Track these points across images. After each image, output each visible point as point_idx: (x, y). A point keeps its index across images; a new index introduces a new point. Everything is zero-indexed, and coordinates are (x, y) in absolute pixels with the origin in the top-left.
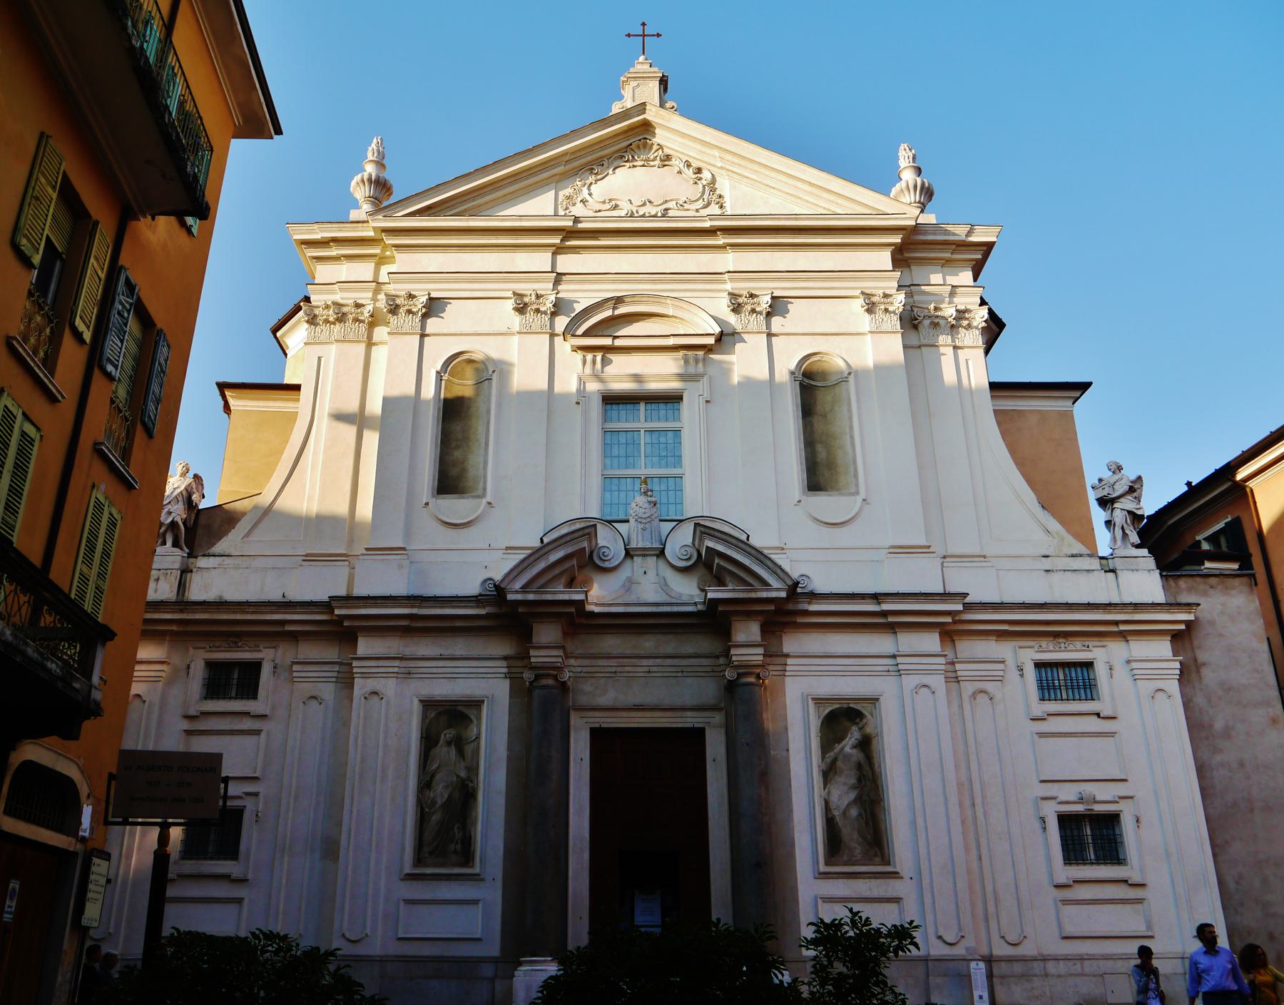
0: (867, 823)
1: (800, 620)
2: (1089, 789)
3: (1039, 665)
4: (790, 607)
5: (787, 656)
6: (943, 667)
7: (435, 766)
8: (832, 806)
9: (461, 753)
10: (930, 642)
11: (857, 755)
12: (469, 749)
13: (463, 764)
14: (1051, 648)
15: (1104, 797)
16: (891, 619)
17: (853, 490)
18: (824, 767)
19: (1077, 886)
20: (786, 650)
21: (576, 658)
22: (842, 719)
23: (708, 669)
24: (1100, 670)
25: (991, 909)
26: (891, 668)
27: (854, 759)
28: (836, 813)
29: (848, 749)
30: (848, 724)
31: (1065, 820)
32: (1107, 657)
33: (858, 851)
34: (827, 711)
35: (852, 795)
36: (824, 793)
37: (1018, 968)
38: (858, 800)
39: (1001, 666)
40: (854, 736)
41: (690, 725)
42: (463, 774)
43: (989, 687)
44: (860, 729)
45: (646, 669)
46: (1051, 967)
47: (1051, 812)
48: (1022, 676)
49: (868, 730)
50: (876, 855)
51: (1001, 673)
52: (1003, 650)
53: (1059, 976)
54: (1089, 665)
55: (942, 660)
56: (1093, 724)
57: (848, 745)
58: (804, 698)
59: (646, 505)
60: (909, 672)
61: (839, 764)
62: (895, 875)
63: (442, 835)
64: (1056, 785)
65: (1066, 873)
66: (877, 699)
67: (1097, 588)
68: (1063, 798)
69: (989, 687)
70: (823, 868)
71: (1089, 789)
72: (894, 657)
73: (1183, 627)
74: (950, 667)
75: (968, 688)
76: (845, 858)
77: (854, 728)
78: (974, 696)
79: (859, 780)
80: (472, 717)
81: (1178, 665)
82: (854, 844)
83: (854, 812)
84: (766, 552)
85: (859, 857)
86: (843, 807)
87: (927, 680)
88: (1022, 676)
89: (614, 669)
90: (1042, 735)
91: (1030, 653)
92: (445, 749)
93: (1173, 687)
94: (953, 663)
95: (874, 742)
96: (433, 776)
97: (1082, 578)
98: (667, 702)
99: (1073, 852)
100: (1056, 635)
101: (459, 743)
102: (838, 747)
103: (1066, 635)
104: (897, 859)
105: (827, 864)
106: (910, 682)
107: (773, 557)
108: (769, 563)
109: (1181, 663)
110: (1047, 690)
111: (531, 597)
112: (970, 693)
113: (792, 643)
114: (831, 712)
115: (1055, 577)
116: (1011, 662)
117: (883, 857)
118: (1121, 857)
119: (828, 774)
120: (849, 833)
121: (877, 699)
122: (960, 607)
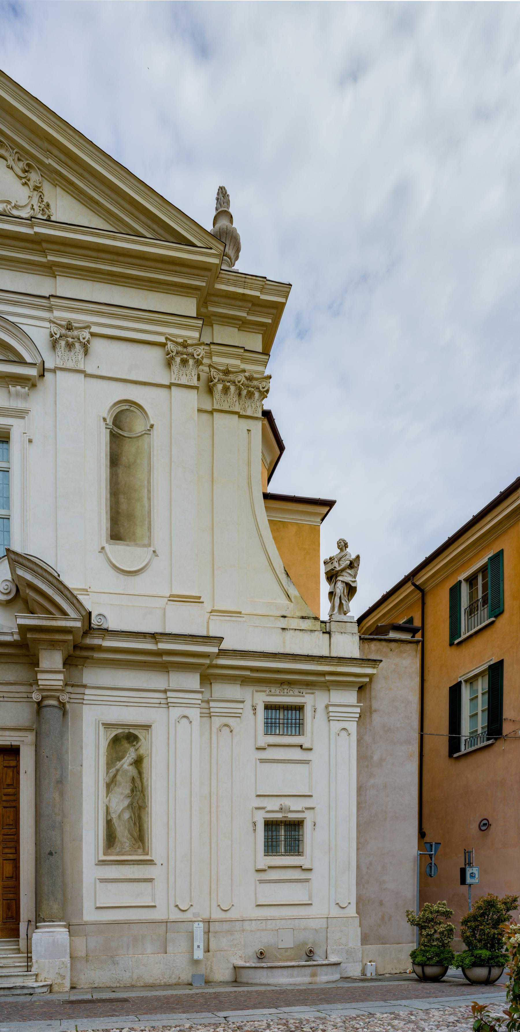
0: (135, 824)
1: (97, 655)
2: (287, 802)
3: (268, 707)
5: (85, 686)
6: (199, 702)
8: (111, 810)
10: (192, 681)
11: (132, 771)
14: (278, 693)
15: (295, 808)
16: (166, 658)
17: (146, 541)
18: (108, 780)
20: (85, 682)
24: (308, 711)
25: (214, 887)
26: (163, 701)
27: (130, 774)
28: (114, 816)
31: (270, 825)
32: (313, 702)
34: (113, 735)
35: (127, 802)
37: (226, 926)
38: (131, 806)
39: (241, 705)
41: (9, 743)
44: (136, 750)
46: (247, 925)
48: (255, 714)
49: (141, 751)
50: (139, 848)
51: (240, 711)
53: (251, 931)
54: (300, 708)
55: (199, 696)
56: (297, 754)
61: (118, 778)
62: (151, 862)
64: (266, 799)
65: (264, 861)
66: (150, 726)
67: (315, 644)
68: (269, 808)
71: (287, 802)
72: (165, 691)
73: (367, 680)
74: (204, 705)
76: (118, 850)
77: (132, 749)
79: (132, 791)
81: (358, 710)
83: (127, 815)
84: (75, 593)
86: (119, 811)
87: (187, 712)
88: (255, 714)
90: (262, 761)
91: (261, 697)
93: (353, 727)
94: (208, 702)
99: (271, 847)
100: (282, 683)
102: (119, 764)
103: (290, 683)
104: (153, 851)
105: (105, 854)
106: (175, 712)
107: (79, 597)
108: (75, 602)
110: (270, 726)
112: (218, 726)
113: (92, 676)
114: (116, 735)
115: (289, 634)
117: (144, 849)
118: (300, 851)
119: (110, 785)
120: (122, 833)
121: (150, 726)
122: (217, 651)
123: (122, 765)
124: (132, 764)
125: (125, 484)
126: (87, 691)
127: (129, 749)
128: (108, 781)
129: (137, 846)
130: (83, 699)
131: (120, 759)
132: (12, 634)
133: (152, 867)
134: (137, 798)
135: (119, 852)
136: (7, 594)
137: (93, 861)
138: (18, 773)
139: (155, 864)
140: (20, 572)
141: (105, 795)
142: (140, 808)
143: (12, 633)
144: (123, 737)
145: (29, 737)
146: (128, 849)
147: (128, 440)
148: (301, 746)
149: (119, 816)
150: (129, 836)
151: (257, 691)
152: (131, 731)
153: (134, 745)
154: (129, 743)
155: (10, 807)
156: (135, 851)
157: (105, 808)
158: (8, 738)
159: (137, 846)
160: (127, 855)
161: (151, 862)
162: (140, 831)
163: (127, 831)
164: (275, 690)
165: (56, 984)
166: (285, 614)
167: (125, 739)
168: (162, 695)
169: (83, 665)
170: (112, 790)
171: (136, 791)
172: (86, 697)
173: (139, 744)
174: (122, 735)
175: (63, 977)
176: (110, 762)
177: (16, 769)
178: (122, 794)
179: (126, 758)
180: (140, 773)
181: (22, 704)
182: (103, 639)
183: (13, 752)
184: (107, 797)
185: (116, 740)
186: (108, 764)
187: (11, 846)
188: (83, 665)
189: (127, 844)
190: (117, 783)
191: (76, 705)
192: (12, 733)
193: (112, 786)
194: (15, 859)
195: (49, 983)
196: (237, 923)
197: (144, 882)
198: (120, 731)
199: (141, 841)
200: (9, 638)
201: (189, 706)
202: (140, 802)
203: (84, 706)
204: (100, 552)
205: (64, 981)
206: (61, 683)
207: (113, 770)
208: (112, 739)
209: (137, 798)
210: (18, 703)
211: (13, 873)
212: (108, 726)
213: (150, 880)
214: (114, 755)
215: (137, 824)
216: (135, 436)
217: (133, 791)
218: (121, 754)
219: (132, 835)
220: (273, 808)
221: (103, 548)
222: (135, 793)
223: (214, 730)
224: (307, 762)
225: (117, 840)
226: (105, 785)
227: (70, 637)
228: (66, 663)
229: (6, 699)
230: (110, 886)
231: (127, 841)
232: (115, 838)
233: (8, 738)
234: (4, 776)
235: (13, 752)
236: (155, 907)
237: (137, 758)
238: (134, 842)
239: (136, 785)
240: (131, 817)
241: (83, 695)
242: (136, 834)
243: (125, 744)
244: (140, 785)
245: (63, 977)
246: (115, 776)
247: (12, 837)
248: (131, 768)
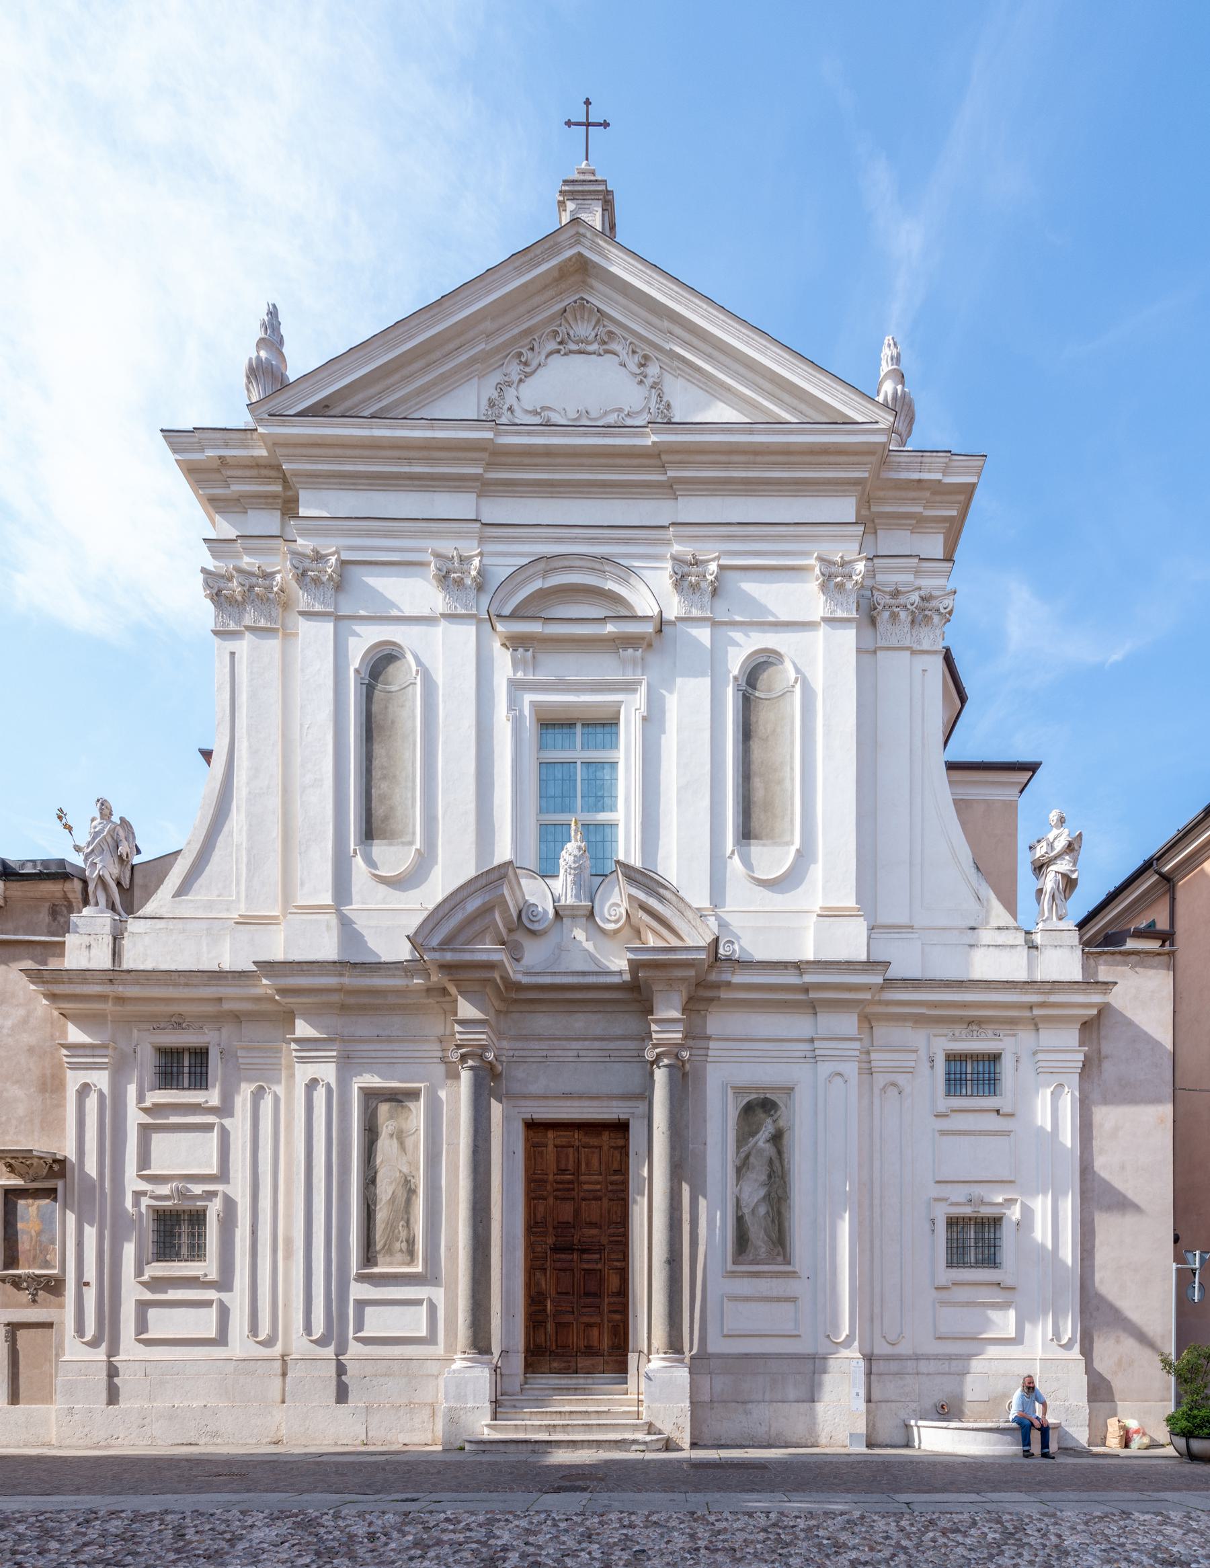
0: (773, 1221)
1: (724, 994)
2: (977, 1190)
3: (952, 1058)
4: (713, 977)
5: (709, 1038)
6: (857, 1053)
8: (743, 1203)
11: (769, 1149)
16: (812, 995)
18: (738, 1163)
19: (955, 1288)
20: (709, 1032)
22: (759, 1109)
25: (877, 1310)
26: (809, 1054)
27: (767, 1154)
28: (746, 1211)
29: (761, 1144)
30: (763, 1116)
31: (953, 1222)
34: (745, 1102)
36: (736, 1190)
37: (894, 1366)
38: (767, 1197)
39: (913, 1056)
40: (767, 1129)
43: (901, 1079)
44: (774, 1122)
46: (924, 1366)
47: (941, 1213)
48: (932, 1067)
49: (781, 1123)
50: (778, 1254)
51: (912, 1064)
52: (916, 1037)
53: (928, 1374)
54: (995, 1058)
55: (857, 1045)
57: (761, 1139)
58: (725, 1086)
60: (826, 1058)
61: (752, 1159)
62: (793, 1274)
64: (949, 1186)
65: (946, 1276)
68: (953, 1199)
69: (901, 1079)
70: (730, 1267)
71: (977, 1190)
72: (812, 1040)
74: (864, 1056)
75: (880, 1080)
77: (769, 1121)
78: (884, 1089)
79: (770, 1177)
82: (760, 1243)
83: (762, 1210)
85: (763, 1256)
87: (841, 1067)
90: (944, 1133)
95: (786, 1136)
97: (1005, 955)
99: (956, 1255)
100: (971, 1022)
102: (752, 1141)
106: (825, 1069)
109: (1085, 1056)
110: (954, 1084)
112: (882, 1085)
113: (717, 1023)
114: (748, 1103)
116: (923, 1053)
120: (757, 1233)
129: (776, 1252)
131: (753, 1134)
138: (627, 1155)
142: (780, 1199)
148: (998, 1111)
149: (753, 1211)
151: (935, 1035)
152: (768, 1096)
154: (765, 1112)
158: (615, 1110)
161: (793, 1274)
162: (780, 1231)
164: (959, 1030)
166: (973, 924)
167: (759, 1109)
168: (806, 1046)
173: (779, 1113)
178: (756, 1180)
180: (780, 1153)
185: (748, 1110)
186: (738, 1141)
196: (909, 1362)
198: (754, 1096)
201: (843, 1059)
202: (780, 1192)
207: (745, 1149)
212: (739, 1090)
213: (793, 1299)
219: (769, 1237)
220: (958, 1202)
223: (876, 1091)
224: (1007, 1133)
232: (748, 1240)
233: (615, 1110)
242: (774, 1236)
243: (761, 1115)
246: (747, 1157)
248: (768, 1145)
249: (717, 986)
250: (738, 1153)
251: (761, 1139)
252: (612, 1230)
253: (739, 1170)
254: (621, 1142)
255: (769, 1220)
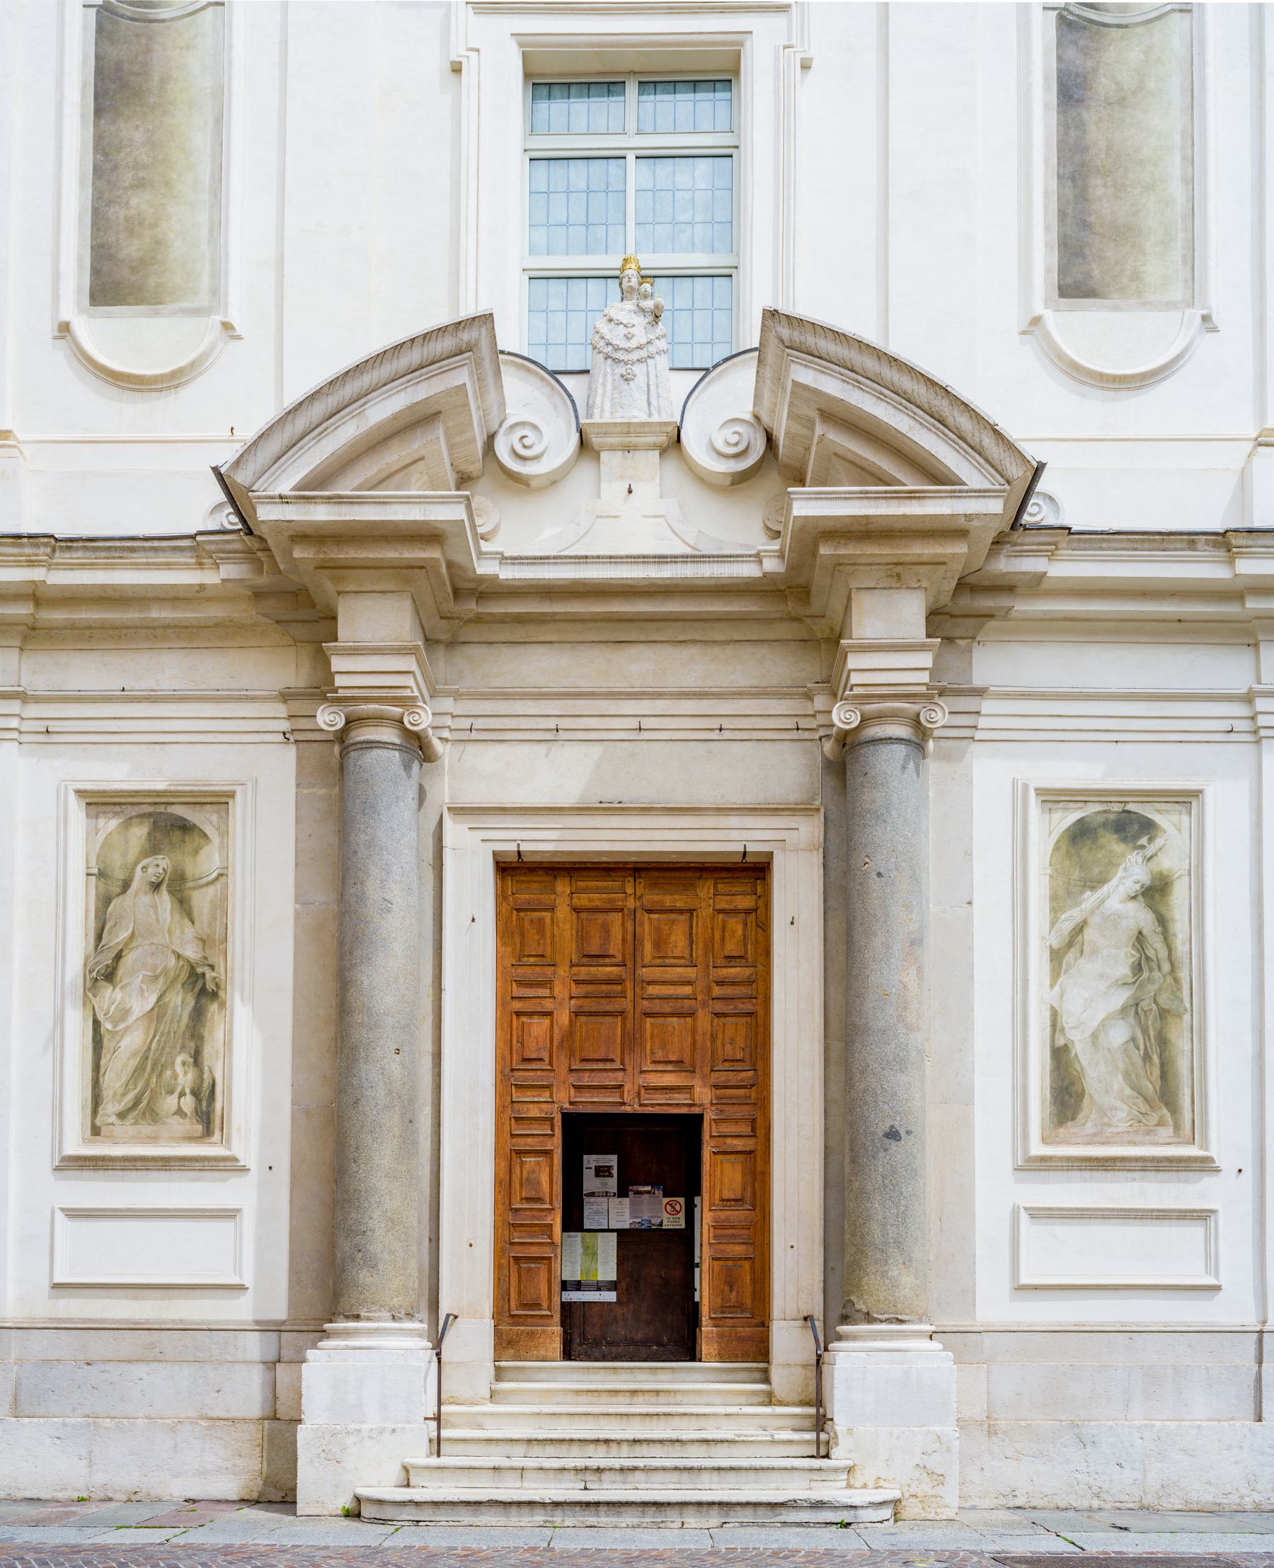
0: (1147, 1057)
4: (1006, 565)
5: (980, 692)
7: (123, 935)
8: (1066, 1021)
9: (183, 904)
12: (202, 900)
13: (190, 931)
21: (457, 696)
23: (790, 723)
30: (1117, 847)
33: (1121, 1117)
35: (1121, 997)
38: (1134, 1008)
40: (1131, 871)
42: (192, 952)
45: (633, 723)
57: (1117, 896)
58: (1019, 793)
59: (640, 321)
61: (1089, 934)
63: (150, 1089)
70: (1038, 1149)
76: (1090, 1128)
79: (1138, 969)
80: (208, 830)
83: (1119, 1034)
86: (1095, 1024)
89: (551, 723)
92: (146, 899)
96: (119, 956)
98: (681, 800)
101: (177, 886)
102: (1090, 898)
105: (1045, 1141)
111: (321, 514)
113: (992, 664)
123: (1103, 901)
124: (1134, 898)
125: (1109, 148)
126: (987, 706)
127: (1124, 856)
128: (1056, 945)
129: (1154, 1118)
130: (975, 727)
131: (1094, 883)
132: (758, 558)
133: (1208, 1181)
134: (1153, 988)
135: (1095, 1135)
136: (736, 456)
137: (1006, 1162)
138: (764, 926)
139: (1217, 1170)
140: (804, 375)
141: (1047, 981)
142: (1163, 1014)
143: (757, 555)
144: (1105, 825)
145: (803, 829)
146: (1123, 1127)
147: (1114, 33)
149: (1095, 1036)
150: (1128, 1091)
152: (1131, 807)
153: (1142, 847)
154: (1124, 840)
155: (736, 1015)
156: (1148, 1133)
157: (1048, 1014)
159: (1154, 1118)
160: (1122, 1143)
161: (1204, 1165)
162: (1164, 1076)
163: (1120, 1077)
165: (915, 1496)
169: (973, 638)
170: (1069, 967)
171: (1151, 970)
172: (982, 722)
173: (1159, 842)
174: (1100, 819)
175: (939, 1479)
176: (1061, 892)
177: (759, 920)
179: (1114, 882)
181: (777, 746)
182: (1051, 556)
183: (753, 871)
184: (1052, 986)
185: (1080, 834)
186: (1054, 898)
187: (738, 1115)
188: (973, 638)
189: (1122, 1114)
190: (1086, 949)
191: (951, 743)
192: (749, 821)
193: (1071, 955)
194: (751, 1152)
195: (895, 1494)
197: (1178, 1218)
199: (1167, 1105)
200: (748, 571)
203: (975, 747)
204: (1023, 333)
205: (940, 1490)
206: (924, 677)
207: (1072, 916)
208: (1068, 830)
209: (1153, 988)
210: (767, 744)
211: (744, 1189)
212: (1053, 798)
213: (1202, 1216)
214: (1076, 874)
215: (1156, 1059)
216: (1139, 19)
217: (1141, 970)
218: (1096, 870)
221: (1036, 321)
222: (1145, 975)
225: (1086, 1101)
226: (1047, 955)
227: (961, 548)
228: (937, 618)
229: (727, 735)
230: (1063, 1230)
231: (1119, 1104)
232: (1081, 1095)
233: (735, 835)
234: (717, 936)
235: (753, 871)
236: (1217, 1288)
237: (1153, 879)
238: (1144, 1108)
239: (1151, 953)
240: (1133, 1039)
241: (973, 717)
242: (1150, 1088)
243: (1112, 844)
244: (1163, 953)
245: (939, 1479)
246: (1080, 929)
247: (742, 1092)
248: (1132, 907)
249: (1007, 587)
250: (1053, 923)
251: (1117, 896)
252: (722, 1078)
253: (1057, 957)
254: (745, 902)
255: (1137, 1057)
